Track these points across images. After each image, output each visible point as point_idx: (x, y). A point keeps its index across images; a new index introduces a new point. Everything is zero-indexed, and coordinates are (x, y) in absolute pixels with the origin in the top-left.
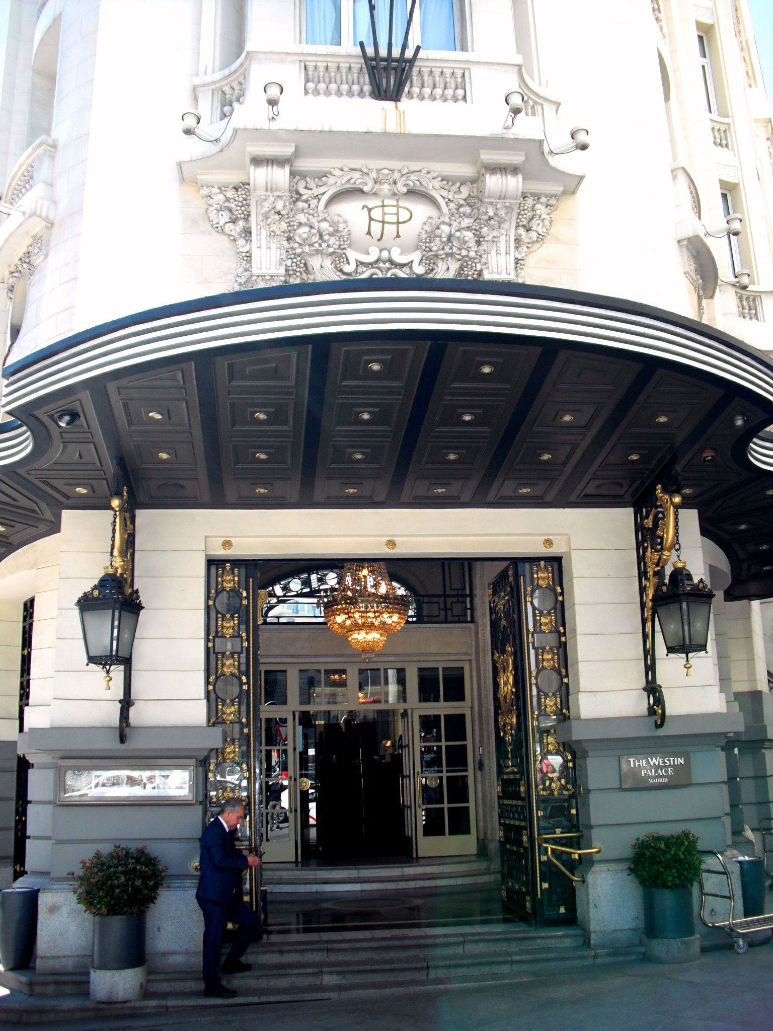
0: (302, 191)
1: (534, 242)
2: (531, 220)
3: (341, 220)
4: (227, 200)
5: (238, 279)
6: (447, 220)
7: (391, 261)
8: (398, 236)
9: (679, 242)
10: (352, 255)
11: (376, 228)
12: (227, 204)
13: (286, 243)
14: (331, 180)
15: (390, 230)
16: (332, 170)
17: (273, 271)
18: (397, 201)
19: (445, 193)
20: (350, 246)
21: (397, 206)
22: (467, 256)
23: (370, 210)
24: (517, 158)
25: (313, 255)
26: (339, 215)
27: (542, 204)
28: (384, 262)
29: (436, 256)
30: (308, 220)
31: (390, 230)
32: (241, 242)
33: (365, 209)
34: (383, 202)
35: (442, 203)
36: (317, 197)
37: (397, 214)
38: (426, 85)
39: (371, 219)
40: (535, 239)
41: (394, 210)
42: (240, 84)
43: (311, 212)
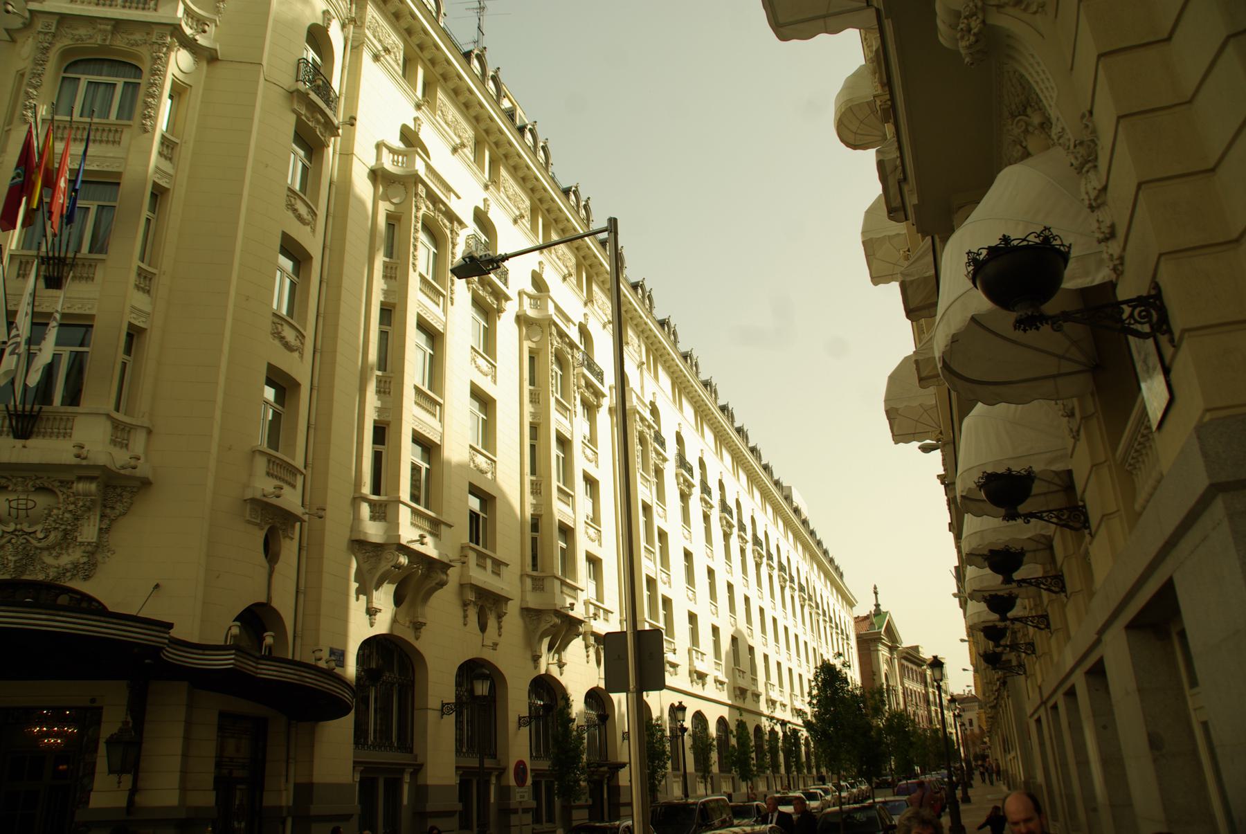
11: (14, 512)
15: (22, 513)
24: (96, 473)
31: (22, 513)
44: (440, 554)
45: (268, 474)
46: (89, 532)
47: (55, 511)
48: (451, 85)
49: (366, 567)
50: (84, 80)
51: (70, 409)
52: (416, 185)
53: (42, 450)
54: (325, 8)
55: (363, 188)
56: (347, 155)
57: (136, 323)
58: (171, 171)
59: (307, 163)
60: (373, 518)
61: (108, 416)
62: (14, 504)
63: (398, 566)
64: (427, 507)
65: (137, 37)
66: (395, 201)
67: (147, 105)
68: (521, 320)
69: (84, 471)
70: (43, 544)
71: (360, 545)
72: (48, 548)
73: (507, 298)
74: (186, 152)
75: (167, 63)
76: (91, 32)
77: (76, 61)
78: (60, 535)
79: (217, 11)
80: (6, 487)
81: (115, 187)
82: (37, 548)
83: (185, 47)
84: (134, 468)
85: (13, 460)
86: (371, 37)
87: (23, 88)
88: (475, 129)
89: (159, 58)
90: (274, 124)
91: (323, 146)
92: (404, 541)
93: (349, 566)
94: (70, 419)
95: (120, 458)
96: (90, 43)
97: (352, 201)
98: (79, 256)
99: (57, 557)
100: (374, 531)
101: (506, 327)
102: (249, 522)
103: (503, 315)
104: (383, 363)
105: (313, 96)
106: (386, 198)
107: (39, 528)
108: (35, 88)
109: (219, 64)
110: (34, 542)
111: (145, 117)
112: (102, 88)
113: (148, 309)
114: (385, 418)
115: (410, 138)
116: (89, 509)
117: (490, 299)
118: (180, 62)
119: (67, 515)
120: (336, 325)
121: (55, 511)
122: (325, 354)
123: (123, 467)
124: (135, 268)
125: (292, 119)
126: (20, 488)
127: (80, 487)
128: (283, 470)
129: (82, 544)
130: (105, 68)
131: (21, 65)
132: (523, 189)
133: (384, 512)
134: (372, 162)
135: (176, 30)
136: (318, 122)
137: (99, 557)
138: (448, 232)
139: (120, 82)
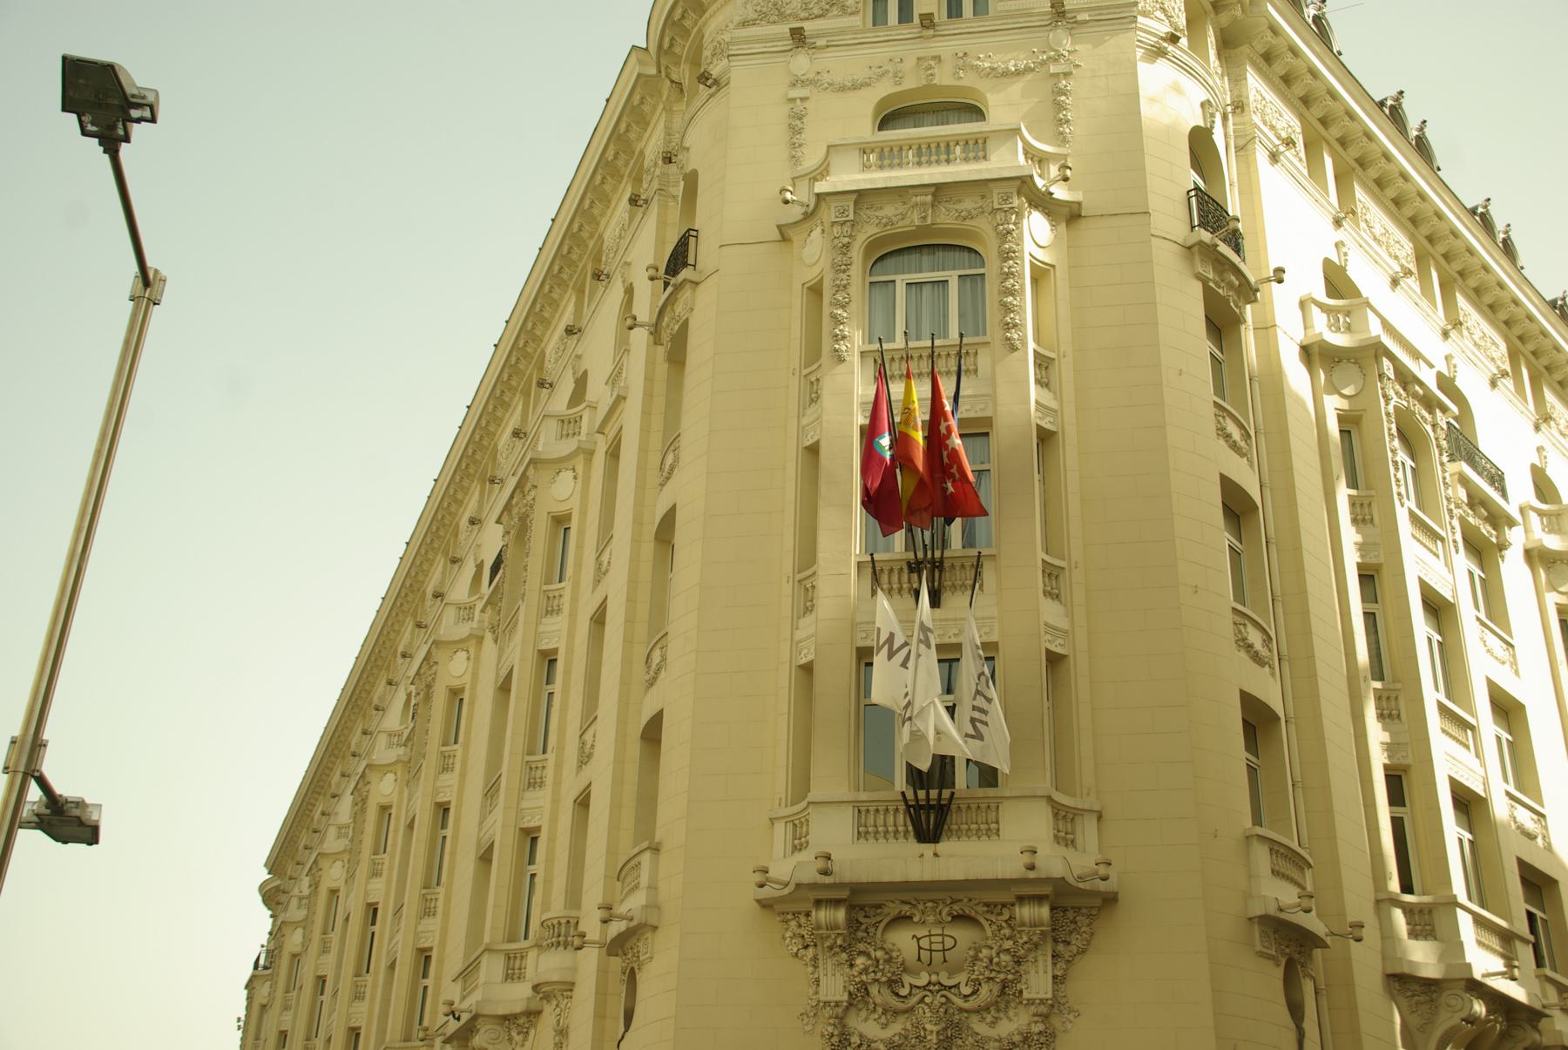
0: (862, 920)
6: (990, 942)
10: (907, 979)
11: (925, 955)
15: (938, 956)
19: (989, 916)
20: (905, 970)
24: (1047, 890)
31: (938, 956)
35: (986, 924)
36: (876, 925)
41: (939, 939)
44: (1529, 994)
45: (1275, 873)
46: (1038, 982)
47: (985, 952)
48: (1373, 173)
49: (1415, 1020)
50: (901, 281)
51: (991, 792)
52: (1377, 358)
53: (957, 858)
54: (1205, 96)
55: (1297, 378)
56: (1266, 329)
57: (1052, 648)
58: (1054, 405)
59: (1217, 352)
60: (1413, 934)
61: (1049, 798)
62: (925, 943)
63: (1471, 1020)
64: (1482, 906)
65: (968, 204)
67: (1007, 309)
68: (1536, 557)
69: (1027, 889)
70: (972, 1003)
71: (1402, 983)
72: (977, 1011)
73: (1511, 523)
74: (1065, 371)
75: (1021, 238)
76: (902, 209)
77: (890, 253)
78: (996, 989)
79: (1062, 139)
80: (910, 918)
81: (984, 439)
82: (961, 1010)
83: (1036, 207)
84: (1105, 879)
85: (927, 877)
86: (1260, 124)
87: (826, 310)
88: (1412, 238)
89: (1009, 232)
90: (1183, 305)
91: (1238, 320)
92: (1477, 975)
93: (1392, 1022)
94: (994, 806)
95: (1054, 862)
96: (902, 226)
97: (1290, 404)
98: (947, 554)
99: (993, 1024)
100: (1422, 957)
101: (1514, 571)
102: (1261, 954)
103: (1506, 553)
104: (1378, 671)
105: (1224, 249)
106: (1333, 389)
107: (962, 978)
108: (843, 307)
109: (1083, 223)
110: (959, 1002)
111: (1008, 327)
112: (927, 290)
113: (1063, 624)
114: (1400, 760)
115: (1337, 282)
116: (1036, 946)
117: (1486, 529)
118: (1036, 233)
119: (1005, 958)
120: (1305, 612)
121: (985, 952)
122: (1294, 658)
123: (1080, 878)
124: (1040, 563)
125: (1197, 288)
126: (931, 918)
127: (1026, 912)
128: (1289, 861)
129: (1031, 1002)
130: (926, 259)
131: (810, 275)
132: (1492, 323)
133: (1427, 922)
134: (1300, 336)
135: (1023, 184)
136: (1231, 286)
137: (1056, 1022)
138: (1429, 428)
139: (952, 277)
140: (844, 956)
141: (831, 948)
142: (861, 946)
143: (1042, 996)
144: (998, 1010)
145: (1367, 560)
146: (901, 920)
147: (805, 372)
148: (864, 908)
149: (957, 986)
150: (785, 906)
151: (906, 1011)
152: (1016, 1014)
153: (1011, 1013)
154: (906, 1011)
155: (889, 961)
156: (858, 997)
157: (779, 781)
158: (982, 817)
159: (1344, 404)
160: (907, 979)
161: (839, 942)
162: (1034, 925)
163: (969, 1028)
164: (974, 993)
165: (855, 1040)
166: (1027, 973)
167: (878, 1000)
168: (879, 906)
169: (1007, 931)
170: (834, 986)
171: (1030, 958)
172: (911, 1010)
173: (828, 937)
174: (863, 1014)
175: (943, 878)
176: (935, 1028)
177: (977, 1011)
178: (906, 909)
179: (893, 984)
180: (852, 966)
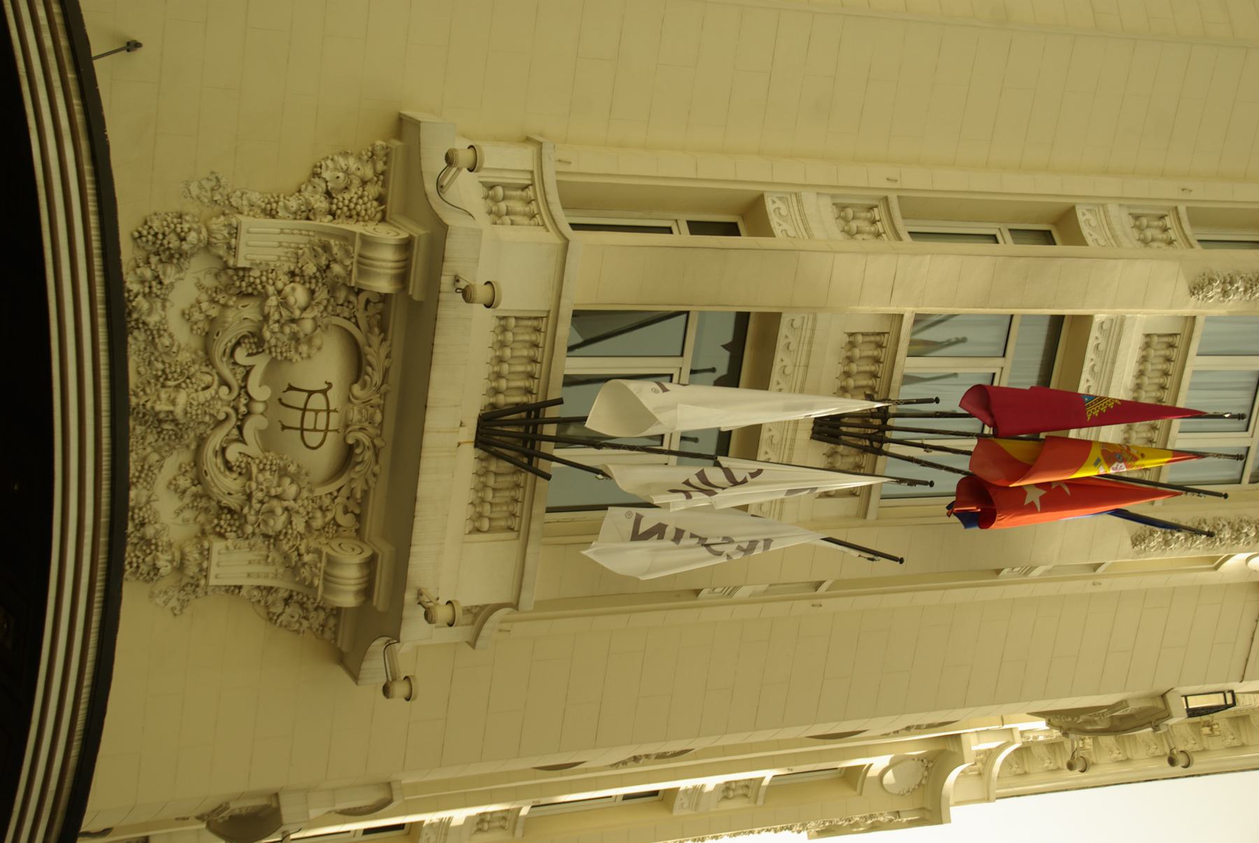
1: (267, 607)
2: (302, 605)
3: (314, 351)
4: (364, 183)
5: (238, 193)
6: (305, 494)
7: (249, 413)
8: (284, 427)
9: (277, 795)
10: (260, 363)
11: (298, 399)
12: (356, 182)
13: (286, 269)
14: (375, 340)
16: (388, 343)
17: (242, 250)
18: (336, 431)
19: (344, 492)
20: (274, 360)
21: (327, 430)
22: (246, 522)
23: (324, 392)
24: (380, 600)
25: (262, 309)
26: (319, 349)
27: (326, 619)
28: (247, 405)
29: (250, 479)
30: (319, 303)
31: (294, 418)
32: (293, 204)
33: (326, 386)
34: (335, 411)
35: (333, 487)
36: (352, 318)
37: (315, 430)
38: (500, 479)
39: (311, 393)
40: (272, 610)
41: (321, 425)
42: (533, 216)
43: (330, 308)
47: (292, 490)
53: (450, 466)
62: (317, 402)
66: (889, 777)
70: (211, 461)
72: (197, 461)
78: (233, 502)
82: (202, 441)
99: (172, 485)
107: (253, 448)
110: (215, 441)
121: (292, 490)
129: (206, 554)
140: (311, 269)
141: (326, 248)
142: (322, 295)
143: (213, 571)
144: (196, 496)
145: (680, 796)
146: (358, 365)
147: (1182, 209)
148: (394, 324)
149: (241, 439)
150: (397, 161)
151: (207, 350)
152: (185, 521)
153: (188, 514)
154: (207, 350)
155: (295, 338)
156: (237, 282)
157: (595, 162)
158: (501, 512)
159: (874, 772)
160: (260, 363)
161: (337, 268)
162: (328, 578)
163: (171, 451)
164: (228, 466)
165: (170, 274)
166: (251, 548)
167: (231, 315)
168: (384, 329)
169: (318, 523)
170: (264, 244)
171: (273, 554)
172: (209, 362)
173: (348, 254)
174: (209, 282)
175: (424, 464)
176: (179, 411)
177: (197, 461)
178: (377, 378)
179: (256, 340)
180: (292, 274)
